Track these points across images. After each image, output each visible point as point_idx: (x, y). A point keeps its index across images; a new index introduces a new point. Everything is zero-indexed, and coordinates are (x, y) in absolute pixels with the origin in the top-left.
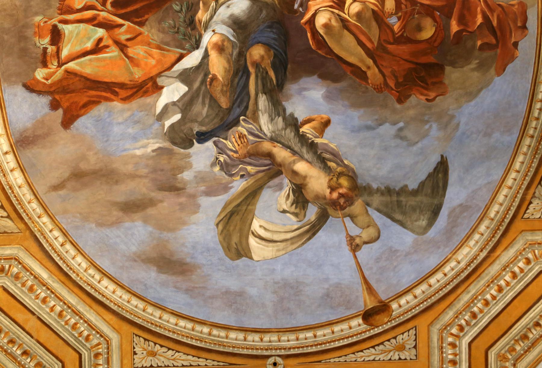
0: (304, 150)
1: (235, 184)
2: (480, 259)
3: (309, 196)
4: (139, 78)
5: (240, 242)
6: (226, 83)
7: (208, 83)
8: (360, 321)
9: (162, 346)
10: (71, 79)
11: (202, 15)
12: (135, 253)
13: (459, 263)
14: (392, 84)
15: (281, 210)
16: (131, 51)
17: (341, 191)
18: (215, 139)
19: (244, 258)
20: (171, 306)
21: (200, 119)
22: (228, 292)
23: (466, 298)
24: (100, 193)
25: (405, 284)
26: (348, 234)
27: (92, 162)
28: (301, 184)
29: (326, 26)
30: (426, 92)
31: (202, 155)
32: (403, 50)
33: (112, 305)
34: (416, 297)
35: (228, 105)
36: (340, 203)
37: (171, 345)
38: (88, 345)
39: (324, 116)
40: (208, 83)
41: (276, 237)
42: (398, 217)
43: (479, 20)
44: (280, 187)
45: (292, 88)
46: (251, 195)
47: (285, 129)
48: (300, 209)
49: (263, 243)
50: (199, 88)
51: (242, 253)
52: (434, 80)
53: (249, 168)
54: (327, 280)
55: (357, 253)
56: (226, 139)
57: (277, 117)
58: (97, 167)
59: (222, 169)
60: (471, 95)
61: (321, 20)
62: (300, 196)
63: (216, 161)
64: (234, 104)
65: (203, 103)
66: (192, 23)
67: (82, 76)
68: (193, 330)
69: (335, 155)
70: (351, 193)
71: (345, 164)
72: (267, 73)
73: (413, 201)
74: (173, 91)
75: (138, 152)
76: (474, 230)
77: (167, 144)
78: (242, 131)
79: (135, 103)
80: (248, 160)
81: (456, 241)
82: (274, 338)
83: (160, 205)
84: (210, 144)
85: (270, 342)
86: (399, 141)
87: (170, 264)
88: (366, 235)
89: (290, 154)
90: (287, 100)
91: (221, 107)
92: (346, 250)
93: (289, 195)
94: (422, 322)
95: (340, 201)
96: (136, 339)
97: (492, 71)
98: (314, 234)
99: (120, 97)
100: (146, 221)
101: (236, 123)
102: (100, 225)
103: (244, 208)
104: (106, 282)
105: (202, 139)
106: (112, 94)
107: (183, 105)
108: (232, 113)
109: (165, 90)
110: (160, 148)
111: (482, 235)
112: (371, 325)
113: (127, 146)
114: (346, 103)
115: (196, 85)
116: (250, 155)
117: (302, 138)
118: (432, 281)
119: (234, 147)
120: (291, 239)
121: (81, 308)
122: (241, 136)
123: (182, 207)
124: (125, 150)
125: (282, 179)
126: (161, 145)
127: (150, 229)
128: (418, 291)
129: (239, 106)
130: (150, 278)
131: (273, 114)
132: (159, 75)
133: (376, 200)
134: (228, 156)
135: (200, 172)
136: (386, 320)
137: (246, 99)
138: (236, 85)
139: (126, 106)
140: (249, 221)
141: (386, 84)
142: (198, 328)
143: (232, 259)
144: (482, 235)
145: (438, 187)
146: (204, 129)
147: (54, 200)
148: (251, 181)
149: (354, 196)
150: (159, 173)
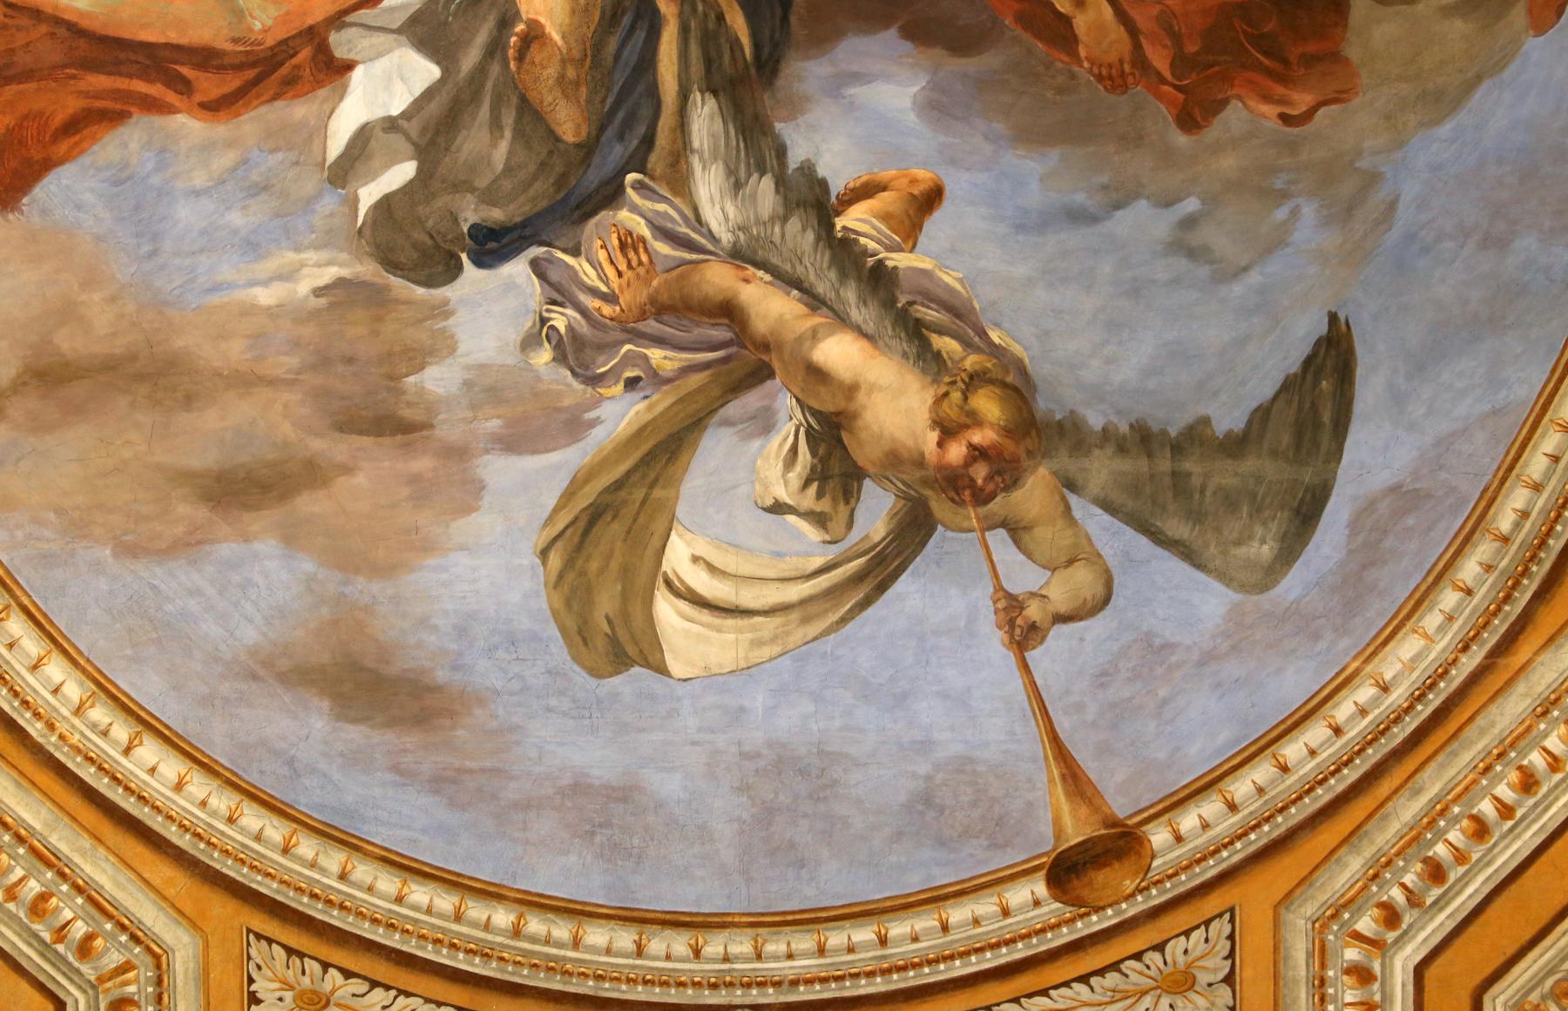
0: (850, 294)
1: (606, 411)
2: (1459, 675)
3: (865, 453)
4: (265, 31)
5: (625, 614)
6: (576, 54)
7: (511, 52)
8: (1041, 888)
9: (348, 974)
10: (19, 29)
12: (253, 652)
13: (1385, 689)
14: (1160, 59)
15: (769, 502)
17: (978, 437)
18: (537, 251)
19: (636, 670)
20: (381, 836)
21: (482, 182)
22: (579, 788)
23: (1408, 810)
24: (128, 438)
25: (1199, 758)
26: (999, 587)
27: (100, 328)
28: (838, 414)
30: (1280, 90)
31: (491, 311)
33: (172, 833)
34: (1232, 807)
35: (584, 134)
36: (973, 480)
37: (381, 970)
38: (86, 969)
39: (921, 173)
40: (511, 52)
41: (749, 597)
42: (1177, 528)
44: (764, 424)
45: (807, 72)
46: (664, 450)
47: (785, 220)
48: (834, 500)
49: (705, 616)
50: (481, 70)
51: (631, 650)
52: (1311, 48)
53: (656, 355)
54: (925, 746)
55: (1034, 656)
56: (575, 252)
57: (755, 176)
58: (119, 347)
59: (560, 357)
60: (1442, 101)
63: (541, 331)
64: (602, 129)
65: (496, 124)
67: (58, 21)
68: (458, 917)
69: (959, 313)
71: (991, 343)
72: (721, 18)
73: (1226, 474)
74: (387, 80)
75: (265, 296)
76: (1440, 575)
77: (367, 269)
78: (630, 225)
79: (253, 122)
80: (651, 326)
81: (1377, 613)
82: (741, 945)
83: (342, 482)
84: (517, 269)
85: (726, 959)
86: (1181, 264)
87: (374, 687)
88: (1061, 590)
89: (801, 309)
90: (791, 117)
91: (558, 139)
92: (994, 645)
93: (794, 449)
94: (1256, 894)
95: (972, 471)
96: (258, 950)
97: (1518, 16)
98: (882, 588)
99: (198, 98)
100: (291, 538)
101: (611, 195)
102: (129, 550)
103: (639, 494)
104: (149, 751)
105: (492, 252)
106: (168, 86)
107: (424, 131)
108: (596, 160)
109: (358, 74)
110: (340, 283)
111: (1469, 592)
112: (1076, 902)
113: (226, 273)
114: (999, 127)
115: (470, 59)
116: (660, 308)
117: (844, 251)
118: (1292, 751)
119: (604, 279)
120: (803, 602)
121: (64, 841)
122: (630, 242)
123: (421, 491)
124: (217, 288)
125: (773, 396)
126: (345, 272)
127: (308, 566)
128: (1241, 787)
129: (621, 137)
130: (306, 738)
131: (743, 167)
132: (338, 20)
133: (1101, 469)
134: (584, 312)
135: (482, 367)
136: (1129, 885)
137: (645, 112)
138: (610, 59)
139: (220, 130)
140: (655, 542)
141: (1141, 62)
142: (476, 910)
143: (596, 673)
144: (1469, 592)
145: (1317, 425)
146: (497, 215)
148: (662, 400)
149: (1023, 456)
150: (340, 369)
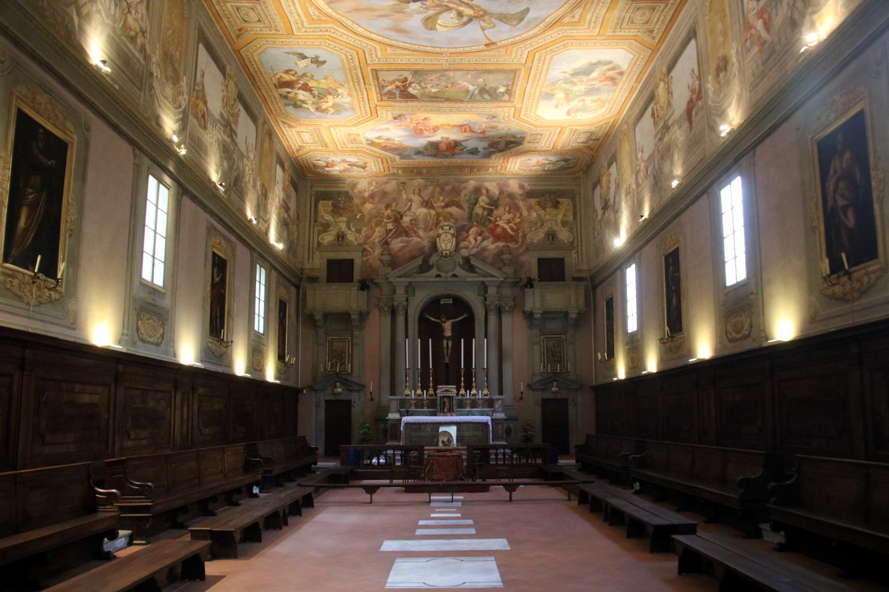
62: (460, 15)
69: (478, 6)
130: (393, 34)
147: (348, 15)
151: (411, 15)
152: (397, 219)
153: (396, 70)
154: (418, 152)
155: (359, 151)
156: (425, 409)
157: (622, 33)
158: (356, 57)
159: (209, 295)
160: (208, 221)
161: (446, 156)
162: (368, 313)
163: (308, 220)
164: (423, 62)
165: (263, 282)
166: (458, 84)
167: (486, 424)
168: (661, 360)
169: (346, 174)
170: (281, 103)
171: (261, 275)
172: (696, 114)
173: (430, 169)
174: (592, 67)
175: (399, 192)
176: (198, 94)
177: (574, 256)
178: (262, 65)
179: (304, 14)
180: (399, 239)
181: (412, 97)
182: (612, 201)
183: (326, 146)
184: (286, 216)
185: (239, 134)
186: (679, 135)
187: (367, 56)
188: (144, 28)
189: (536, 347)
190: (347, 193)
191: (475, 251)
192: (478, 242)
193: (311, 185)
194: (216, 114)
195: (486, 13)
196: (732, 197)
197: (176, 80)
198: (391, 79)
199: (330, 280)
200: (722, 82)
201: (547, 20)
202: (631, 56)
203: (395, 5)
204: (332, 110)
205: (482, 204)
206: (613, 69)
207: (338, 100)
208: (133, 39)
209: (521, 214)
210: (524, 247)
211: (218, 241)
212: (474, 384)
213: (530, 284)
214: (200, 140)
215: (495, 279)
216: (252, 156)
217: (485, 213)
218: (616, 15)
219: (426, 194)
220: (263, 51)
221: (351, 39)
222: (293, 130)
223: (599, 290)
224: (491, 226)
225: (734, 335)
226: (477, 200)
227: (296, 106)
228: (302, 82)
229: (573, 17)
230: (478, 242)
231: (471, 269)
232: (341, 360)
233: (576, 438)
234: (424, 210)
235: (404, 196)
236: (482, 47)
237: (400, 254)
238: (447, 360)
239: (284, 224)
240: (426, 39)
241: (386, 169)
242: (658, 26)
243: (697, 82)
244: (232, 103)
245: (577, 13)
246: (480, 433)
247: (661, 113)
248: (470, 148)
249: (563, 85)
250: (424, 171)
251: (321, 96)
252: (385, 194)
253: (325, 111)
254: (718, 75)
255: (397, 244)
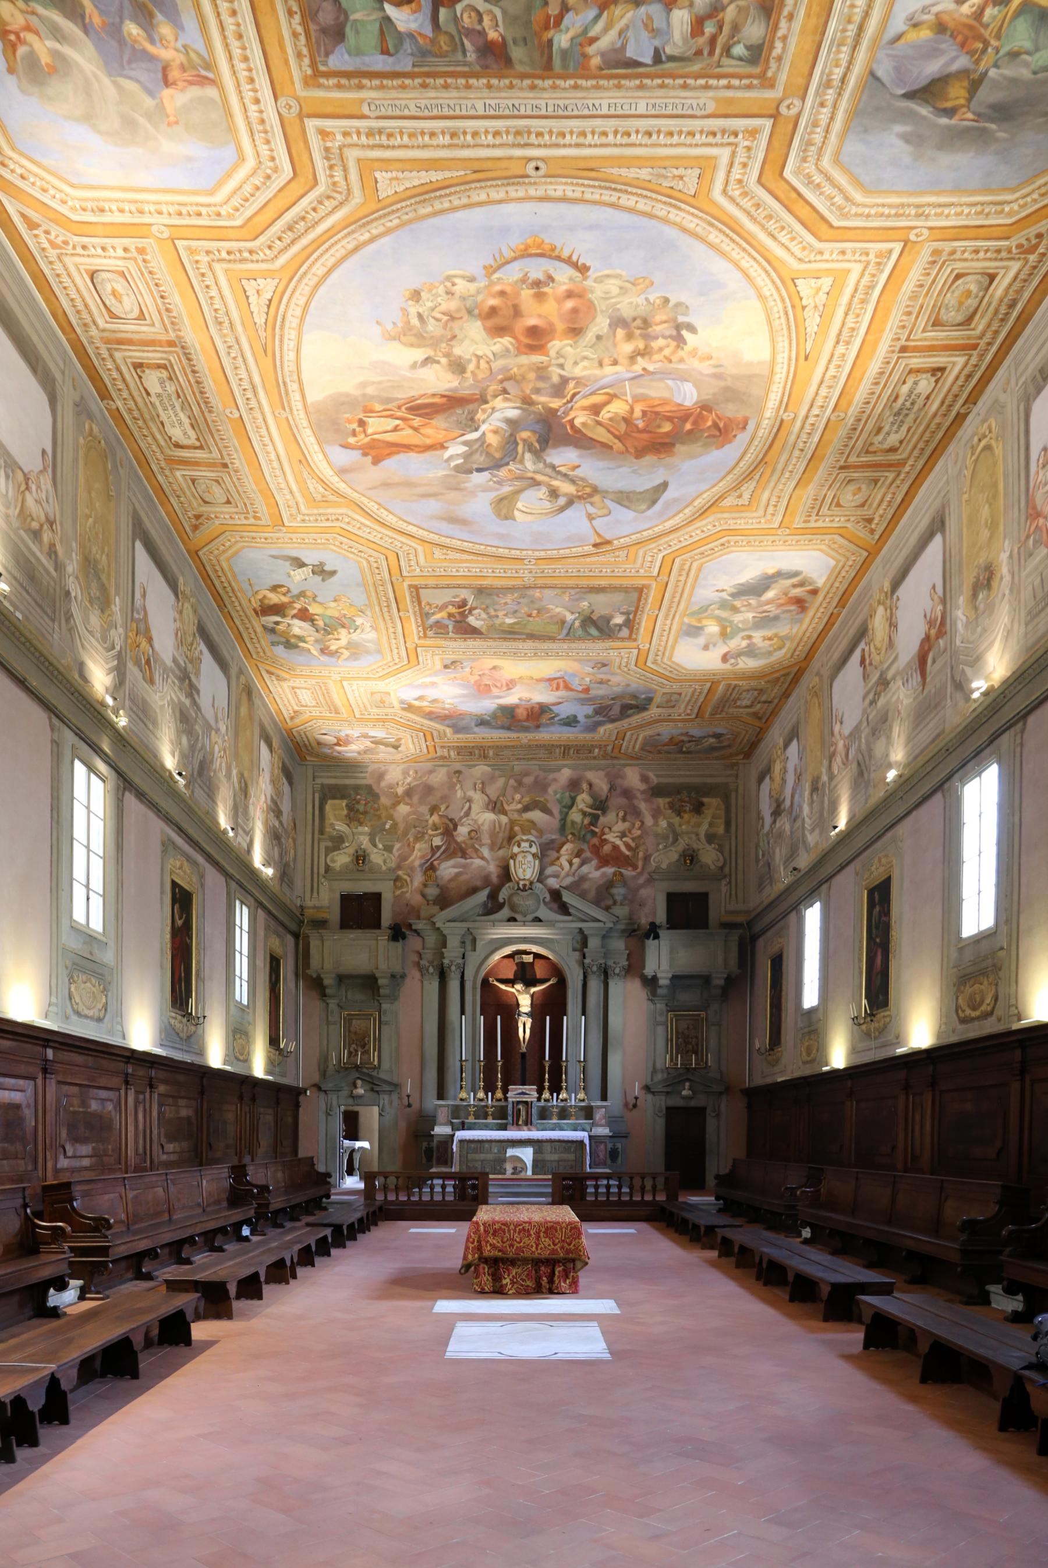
11: (480, 416)
16: (422, 431)
29: (584, 424)
32: (645, 436)
43: (709, 423)
61: (577, 422)
62: (554, 493)
66: (472, 419)
69: (582, 479)
70: (589, 493)
74: (456, 449)
84: (486, 474)
88: (600, 513)
92: (586, 522)
101: (507, 464)
117: (559, 473)
130: (444, 527)
141: (627, 451)
151: (473, 494)
152: (449, 829)
153: (448, 587)
154: (482, 722)
155: (388, 720)
156: (490, 1120)
157: (820, 524)
158: (385, 564)
159: (169, 945)
160: (162, 832)
161: (526, 729)
162: (403, 976)
163: (309, 828)
164: (492, 574)
165: (246, 927)
166: (548, 611)
167: (582, 1142)
168: (853, 1050)
169: (367, 757)
170: (265, 640)
171: (242, 916)
172: (934, 661)
173: (499, 749)
174: (766, 582)
175: (452, 787)
176: (140, 627)
177: (724, 889)
178: (234, 576)
179: (301, 491)
180: (452, 862)
181: (474, 632)
182: (788, 803)
183: (337, 712)
184: (277, 824)
185: (202, 693)
186: (903, 696)
187: (402, 563)
188: (52, 518)
189: (660, 1030)
190: (369, 788)
191: (568, 881)
192: (574, 867)
193: (312, 771)
194: (169, 663)
195: (595, 490)
196: (981, 796)
197: (104, 604)
198: (440, 603)
199: (346, 924)
200: (982, 607)
201: (696, 504)
202: (833, 563)
203: (447, 476)
204: (346, 653)
205: (582, 806)
206: (801, 584)
207: (355, 636)
208: (36, 535)
209: (643, 823)
210: (646, 876)
211: (178, 864)
212: (564, 1084)
213: (653, 931)
214: (145, 702)
215: (601, 925)
216: (223, 729)
217: (586, 821)
218: (812, 493)
219: (493, 791)
220: (236, 553)
221: (377, 534)
222: (285, 684)
223: (761, 942)
224: (595, 841)
225: (968, 1012)
226: (573, 800)
227: (288, 645)
228: (298, 606)
229: (740, 496)
230: (574, 867)
231: (564, 909)
232: (363, 1046)
233: (716, 1165)
234: (489, 816)
235: (459, 794)
236: (589, 549)
237: (452, 885)
238: (524, 1050)
239: (274, 837)
240: (498, 536)
241: (431, 749)
242: (881, 512)
243: (940, 607)
244: (190, 640)
245: (747, 490)
246: (572, 1157)
247: (876, 659)
248: (563, 716)
249: (717, 612)
250: (491, 753)
251: (329, 629)
252: (429, 789)
253: (335, 654)
254: (975, 595)
255: (447, 870)
